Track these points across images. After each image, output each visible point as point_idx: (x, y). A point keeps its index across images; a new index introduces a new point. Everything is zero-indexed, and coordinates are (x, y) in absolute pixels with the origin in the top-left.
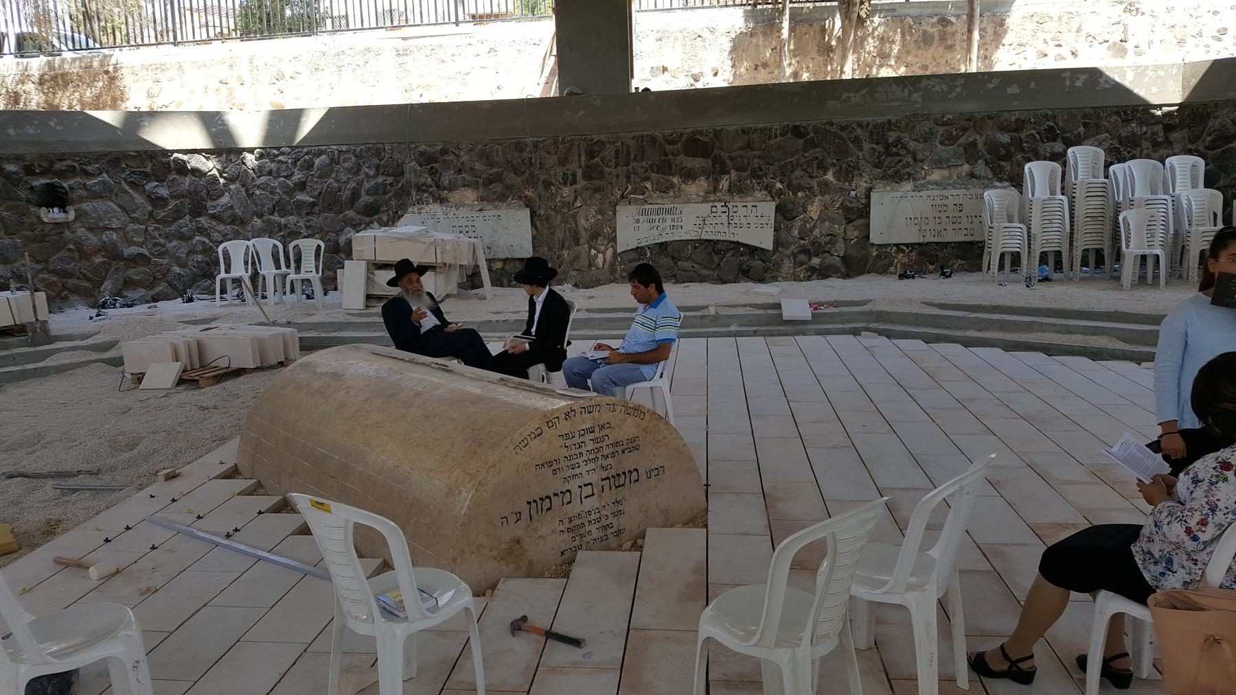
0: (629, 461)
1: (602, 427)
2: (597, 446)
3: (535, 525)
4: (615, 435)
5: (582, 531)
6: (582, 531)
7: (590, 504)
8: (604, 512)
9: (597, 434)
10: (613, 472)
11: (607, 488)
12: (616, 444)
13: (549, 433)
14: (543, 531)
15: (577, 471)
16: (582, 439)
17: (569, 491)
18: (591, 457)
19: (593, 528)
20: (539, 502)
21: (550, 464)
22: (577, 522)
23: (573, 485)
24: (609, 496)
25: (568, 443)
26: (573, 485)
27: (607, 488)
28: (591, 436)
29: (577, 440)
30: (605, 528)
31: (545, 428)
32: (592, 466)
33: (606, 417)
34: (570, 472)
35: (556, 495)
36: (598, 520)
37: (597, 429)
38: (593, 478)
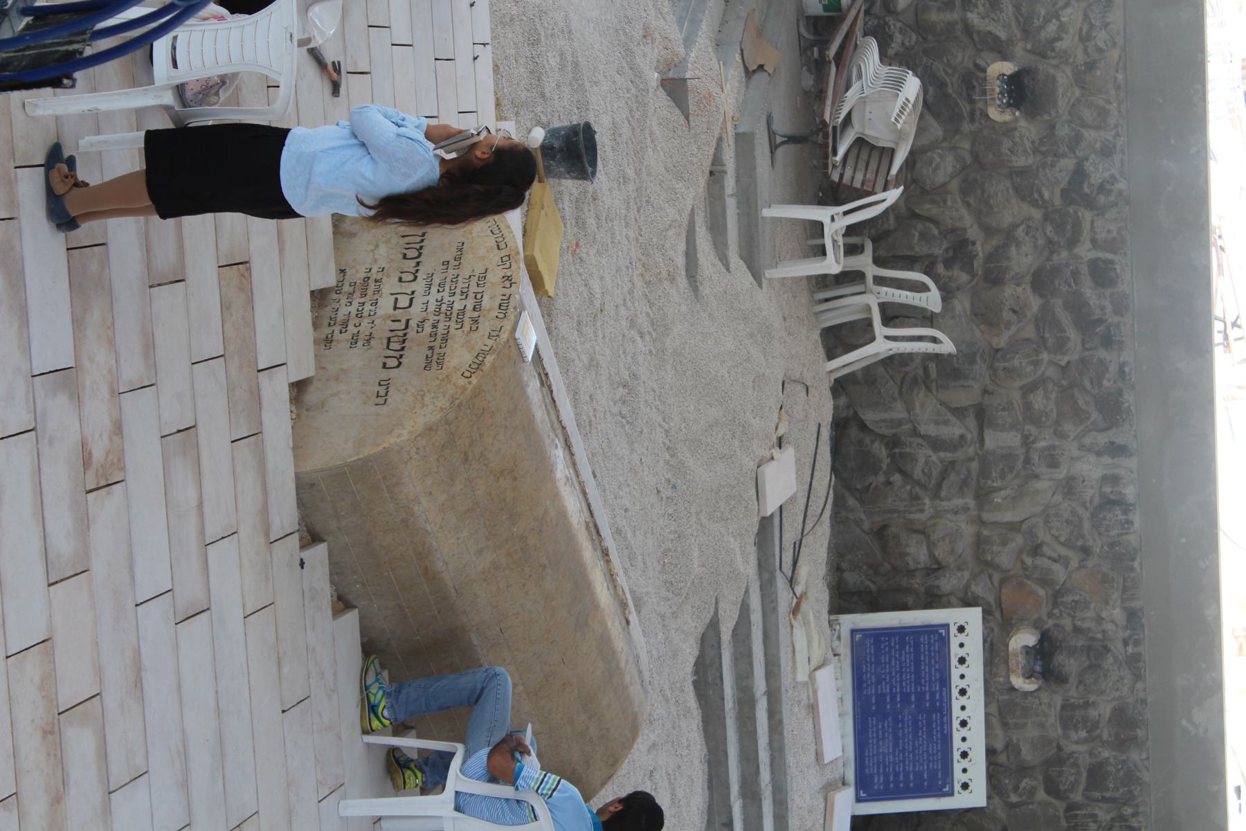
0: (415, 356)
1: (475, 321)
2: (454, 315)
3: (394, 240)
4: (457, 336)
5: (357, 294)
6: (357, 294)
7: (386, 304)
8: (365, 322)
9: (470, 314)
10: (411, 333)
11: (396, 326)
12: (445, 339)
13: (496, 256)
14: (383, 249)
15: (434, 289)
16: (471, 295)
17: (416, 278)
18: (444, 307)
19: (353, 309)
20: (418, 246)
21: (457, 259)
22: (372, 286)
23: (419, 286)
24: (383, 328)
25: (474, 280)
26: (419, 286)
27: (396, 326)
28: (470, 307)
29: (473, 288)
30: (345, 324)
31: (503, 253)
32: (432, 307)
33: (485, 326)
34: (436, 280)
35: (418, 264)
36: (359, 315)
37: (476, 314)
38: (416, 311)
